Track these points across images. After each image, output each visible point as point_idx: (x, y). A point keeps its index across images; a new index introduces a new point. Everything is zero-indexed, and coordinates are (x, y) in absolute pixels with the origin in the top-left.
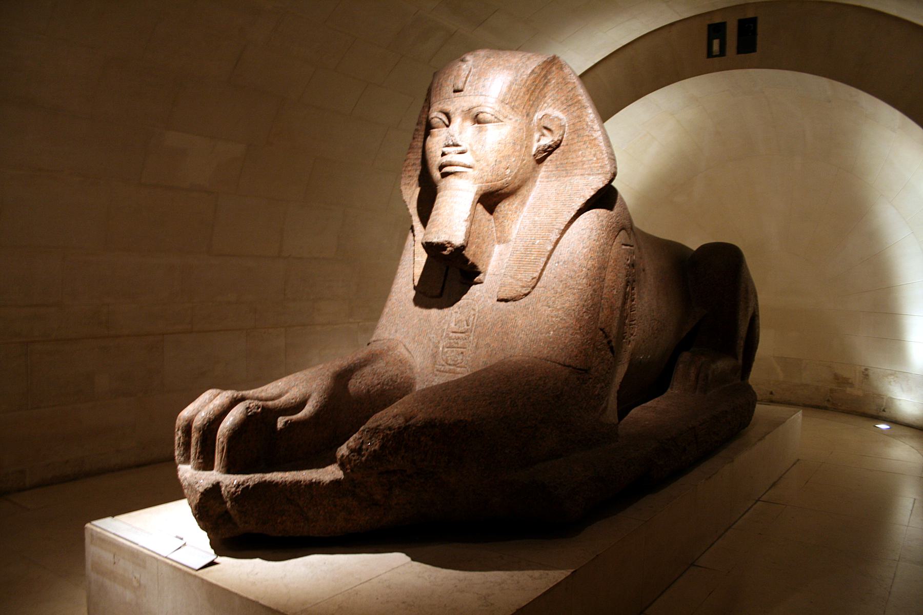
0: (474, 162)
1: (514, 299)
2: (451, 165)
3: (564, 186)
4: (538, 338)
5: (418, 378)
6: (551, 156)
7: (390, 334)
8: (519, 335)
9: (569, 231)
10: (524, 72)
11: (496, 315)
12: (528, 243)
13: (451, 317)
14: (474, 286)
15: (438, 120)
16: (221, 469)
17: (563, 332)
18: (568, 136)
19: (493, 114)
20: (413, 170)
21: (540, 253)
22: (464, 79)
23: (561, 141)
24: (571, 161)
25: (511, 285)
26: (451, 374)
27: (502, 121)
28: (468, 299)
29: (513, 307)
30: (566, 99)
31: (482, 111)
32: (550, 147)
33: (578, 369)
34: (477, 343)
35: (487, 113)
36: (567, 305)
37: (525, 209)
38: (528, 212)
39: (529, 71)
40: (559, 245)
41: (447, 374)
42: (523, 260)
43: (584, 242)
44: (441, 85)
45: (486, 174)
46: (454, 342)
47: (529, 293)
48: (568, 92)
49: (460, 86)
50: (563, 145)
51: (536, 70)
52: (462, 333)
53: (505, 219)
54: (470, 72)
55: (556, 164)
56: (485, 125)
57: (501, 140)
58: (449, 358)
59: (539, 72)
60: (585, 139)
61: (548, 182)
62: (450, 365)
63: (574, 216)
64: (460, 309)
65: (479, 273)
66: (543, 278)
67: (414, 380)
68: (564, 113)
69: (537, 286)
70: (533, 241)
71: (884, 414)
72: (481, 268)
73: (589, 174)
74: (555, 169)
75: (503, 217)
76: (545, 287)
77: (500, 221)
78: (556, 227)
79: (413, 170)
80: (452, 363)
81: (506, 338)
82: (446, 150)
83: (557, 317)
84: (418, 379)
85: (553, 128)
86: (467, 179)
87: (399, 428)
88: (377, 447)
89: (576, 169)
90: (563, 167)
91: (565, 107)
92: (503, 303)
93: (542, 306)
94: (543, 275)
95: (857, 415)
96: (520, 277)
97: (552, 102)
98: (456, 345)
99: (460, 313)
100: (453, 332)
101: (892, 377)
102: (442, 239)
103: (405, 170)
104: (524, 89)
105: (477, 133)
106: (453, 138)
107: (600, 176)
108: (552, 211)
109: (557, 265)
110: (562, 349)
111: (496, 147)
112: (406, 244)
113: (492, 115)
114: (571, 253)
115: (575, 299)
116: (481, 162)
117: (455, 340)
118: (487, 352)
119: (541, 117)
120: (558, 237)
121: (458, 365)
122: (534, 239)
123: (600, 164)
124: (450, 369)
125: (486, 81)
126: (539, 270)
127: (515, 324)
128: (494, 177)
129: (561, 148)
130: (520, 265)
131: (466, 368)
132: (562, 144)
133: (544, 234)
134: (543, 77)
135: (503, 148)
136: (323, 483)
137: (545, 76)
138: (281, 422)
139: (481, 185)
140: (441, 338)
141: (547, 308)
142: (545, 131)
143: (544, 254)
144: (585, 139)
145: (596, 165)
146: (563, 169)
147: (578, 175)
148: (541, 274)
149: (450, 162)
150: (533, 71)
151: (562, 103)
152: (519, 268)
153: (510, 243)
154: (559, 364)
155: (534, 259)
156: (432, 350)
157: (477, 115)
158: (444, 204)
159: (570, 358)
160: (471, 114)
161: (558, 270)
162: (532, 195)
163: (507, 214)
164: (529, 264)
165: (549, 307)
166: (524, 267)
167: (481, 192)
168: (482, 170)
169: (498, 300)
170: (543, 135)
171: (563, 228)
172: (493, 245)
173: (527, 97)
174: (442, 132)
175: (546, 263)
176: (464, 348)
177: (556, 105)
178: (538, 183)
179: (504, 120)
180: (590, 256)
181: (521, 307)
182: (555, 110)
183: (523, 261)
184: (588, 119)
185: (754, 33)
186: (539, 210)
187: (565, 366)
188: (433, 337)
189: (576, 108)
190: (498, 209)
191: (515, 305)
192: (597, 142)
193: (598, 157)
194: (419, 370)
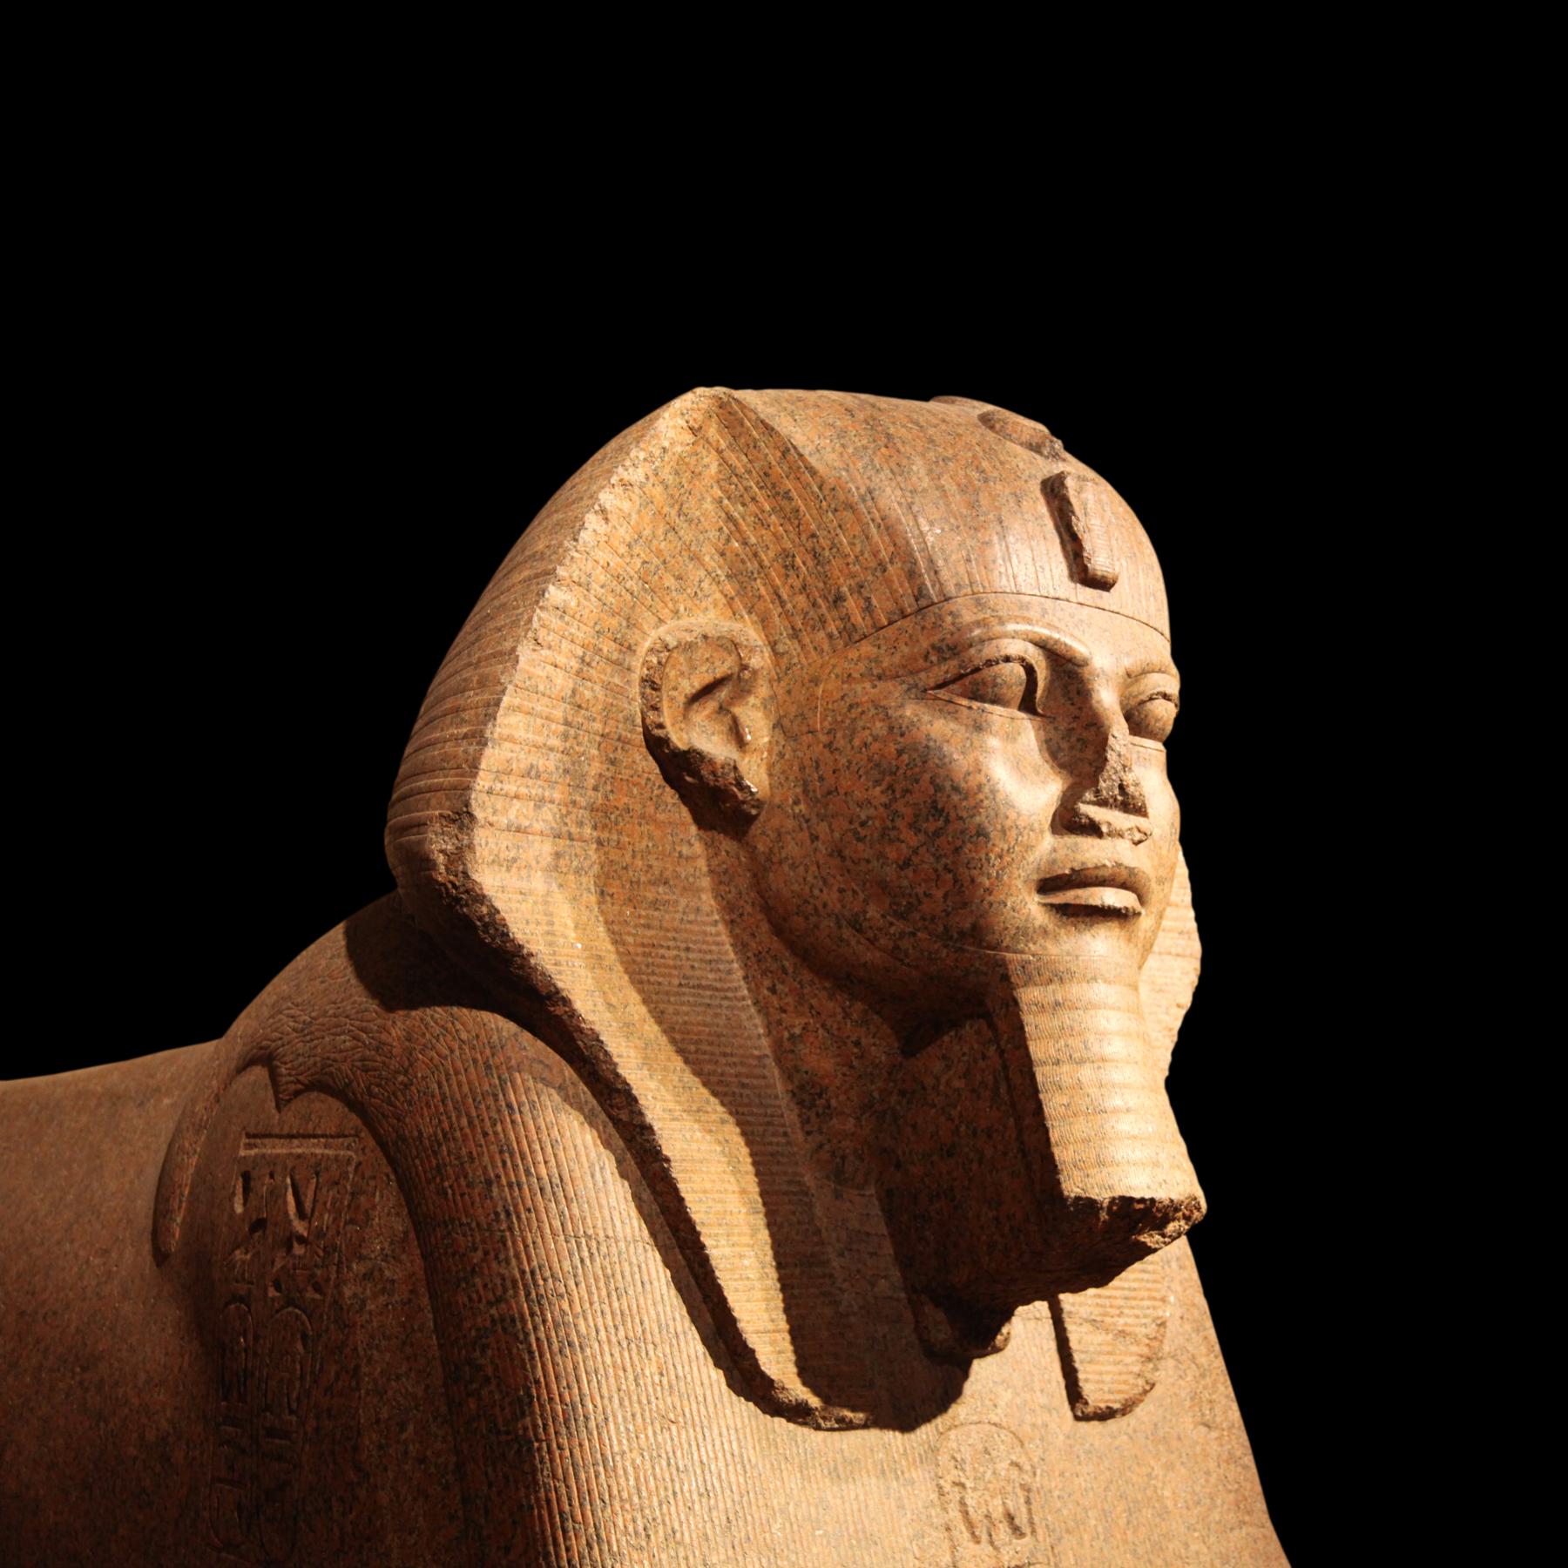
2: (1124, 886)
13: (945, 1510)
15: (1021, 672)
20: (530, 798)
79: (530, 798)
92: (1095, 1423)
93: (1196, 1425)
103: (490, 792)
106: (1129, 778)
107: (1179, 964)
141: (1203, 1429)
149: (1131, 871)
157: (1151, 699)
169: (1077, 1418)
191: (1130, 1430)
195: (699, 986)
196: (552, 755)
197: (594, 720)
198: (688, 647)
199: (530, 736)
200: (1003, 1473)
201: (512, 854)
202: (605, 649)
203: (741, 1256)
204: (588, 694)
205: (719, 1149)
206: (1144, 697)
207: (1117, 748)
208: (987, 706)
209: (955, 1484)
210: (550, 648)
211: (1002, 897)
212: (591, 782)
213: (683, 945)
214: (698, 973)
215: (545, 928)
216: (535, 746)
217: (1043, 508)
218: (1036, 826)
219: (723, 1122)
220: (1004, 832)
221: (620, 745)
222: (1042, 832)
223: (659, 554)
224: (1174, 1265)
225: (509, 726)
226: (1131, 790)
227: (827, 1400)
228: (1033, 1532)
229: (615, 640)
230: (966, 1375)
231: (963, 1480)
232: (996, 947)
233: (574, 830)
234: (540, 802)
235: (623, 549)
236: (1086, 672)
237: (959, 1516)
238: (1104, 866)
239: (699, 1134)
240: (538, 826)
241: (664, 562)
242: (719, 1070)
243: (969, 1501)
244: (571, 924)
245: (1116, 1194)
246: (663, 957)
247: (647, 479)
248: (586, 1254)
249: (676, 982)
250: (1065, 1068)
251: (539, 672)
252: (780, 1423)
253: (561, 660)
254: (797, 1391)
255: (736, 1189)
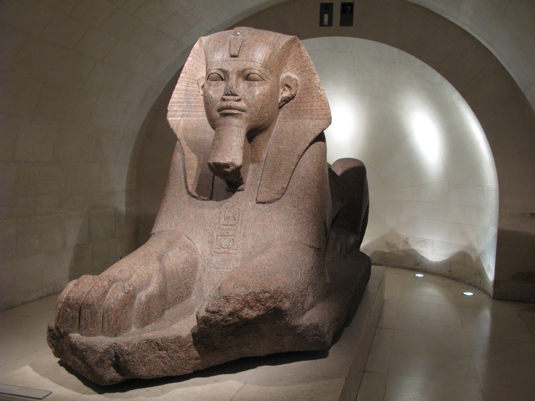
0: (247, 107)
1: (269, 202)
3: (298, 126)
4: (290, 228)
5: (200, 258)
6: (287, 104)
7: (172, 227)
8: (275, 227)
9: (304, 156)
10: (278, 47)
11: (256, 213)
12: (276, 164)
13: (220, 215)
14: (237, 192)
15: (217, 75)
16: (110, 334)
17: (306, 224)
18: (300, 92)
19: (260, 75)
21: (286, 171)
22: (239, 49)
23: (295, 94)
24: (303, 109)
25: (267, 192)
26: (226, 255)
27: (265, 80)
28: (233, 202)
29: (269, 207)
30: (300, 67)
31: (253, 72)
32: (289, 98)
33: (317, 249)
34: (244, 232)
35: (257, 74)
36: (307, 206)
37: (270, 140)
38: (272, 142)
39: (281, 47)
40: (297, 166)
41: (223, 255)
42: (274, 175)
43: (314, 164)
44: (218, 50)
45: (254, 116)
46: (226, 232)
47: (280, 198)
48: (302, 63)
49: (236, 53)
50: (296, 98)
51: (285, 46)
52: (231, 225)
53: (259, 147)
54: (242, 44)
55: (291, 110)
56: (254, 82)
57: (264, 94)
58: (223, 243)
59: (286, 48)
60: (313, 95)
61: (285, 121)
62: (224, 248)
63: (308, 146)
64: (228, 209)
65: (242, 184)
66: (289, 188)
67: (198, 260)
68: (298, 76)
69: (285, 194)
70: (280, 162)
71: (419, 267)
72: (244, 180)
73: (316, 119)
74: (290, 113)
75: (257, 145)
76: (291, 194)
77: (255, 148)
78: (296, 153)
79: (178, 106)
80: (225, 247)
81: (266, 229)
82: (225, 97)
83: (301, 215)
84: (200, 259)
85: (292, 86)
86: (242, 119)
87: (245, 295)
88: (230, 309)
89: (306, 114)
90: (296, 112)
91: (299, 72)
92: (262, 205)
93: (290, 206)
94: (289, 186)
95: (401, 268)
96: (273, 187)
97: (290, 68)
98: (227, 234)
99: (227, 212)
100: (224, 225)
101: (423, 243)
102: (227, 161)
103: (171, 106)
104: (277, 59)
105: (247, 87)
106: (232, 90)
107: (324, 121)
108: (291, 142)
109: (297, 179)
110: (307, 236)
111: (262, 98)
112: (173, 160)
113: (259, 76)
114: (306, 171)
115: (312, 202)
116: (252, 108)
117: (226, 231)
118: (253, 238)
119: (284, 78)
120: (298, 160)
121: (231, 248)
122: (280, 161)
123: (324, 113)
124: (225, 251)
125: (254, 51)
126: (287, 182)
127: (272, 219)
128: (259, 119)
129: (295, 99)
130: (272, 179)
131: (237, 250)
132: (296, 96)
133: (287, 158)
134: (287, 51)
135: (266, 99)
136: (183, 337)
137: (288, 51)
138: (142, 296)
139: (250, 123)
140: (214, 229)
141: (294, 208)
142: (286, 88)
143: (290, 172)
144: (313, 95)
145: (322, 113)
146: (297, 113)
147: (308, 119)
148: (288, 185)
149: (230, 106)
150: (283, 46)
151: (297, 69)
152: (272, 181)
153: (262, 163)
154: (307, 246)
155: (282, 175)
156: (208, 238)
158: (225, 136)
159: (313, 242)
160: (244, 73)
161: (299, 182)
162: (274, 130)
163: (260, 143)
164: (279, 178)
165: (295, 208)
166: (275, 180)
167: (250, 129)
168: (252, 113)
169: (257, 203)
170: (284, 90)
171: (301, 154)
172: (249, 164)
173: (278, 64)
174: (219, 84)
175: (291, 177)
176: (233, 236)
177: (293, 70)
178: (277, 122)
179: (266, 80)
180: (318, 174)
181: (275, 208)
182: (292, 73)
183: (274, 176)
184: (316, 82)
185: (351, 12)
186: (281, 141)
187: (310, 247)
188: (208, 229)
189: (307, 74)
190: (255, 140)
191: (271, 206)
192: (322, 98)
193: (323, 108)
194: (200, 252)
195: (206, 132)
196: (183, 99)
197: (191, 92)
198: (199, 79)
199: (178, 97)
200: (235, 210)
201: (174, 115)
202: (192, 81)
203: (193, 173)
204: (189, 89)
205: (196, 157)
206: (247, 74)
207: (229, 85)
208: (212, 82)
209: (225, 211)
210: (181, 83)
211: (212, 113)
212: (191, 102)
213: (206, 125)
214: (207, 130)
215: (177, 125)
216: (179, 98)
217: (228, 46)
218: (217, 101)
219: (200, 153)
220: (211, 102)
221: (197, 96)
222: (218, 101)
223: (198, 65)
224: (301, 178)
225: (174, 96)
226: (232, 92)
227: (199, 195)
228: (238, 220)
229: (193, 80)
230: (234, 193)
231: (226, 210)
232: (214, 121)
233: (187, 110)
234: (180, 106)
235: (191, 66)
236: (228, 73)
237: (223, 216)
238: (224, 106)
239: (194, 155)
240: (179, 110)
241: (199, 66)
242: (204, 145)
243: (226, 214)
244: (182, 124)
245: (213, 162)
246: (200, 128)
247: (193, 54)
248: (174, 172)
249: (201, 131)
250: (216, 141)
251: (179, 87)
252: (194, 198)
253: (183, 84)
254: (195, 194)
255: (197, 163)
